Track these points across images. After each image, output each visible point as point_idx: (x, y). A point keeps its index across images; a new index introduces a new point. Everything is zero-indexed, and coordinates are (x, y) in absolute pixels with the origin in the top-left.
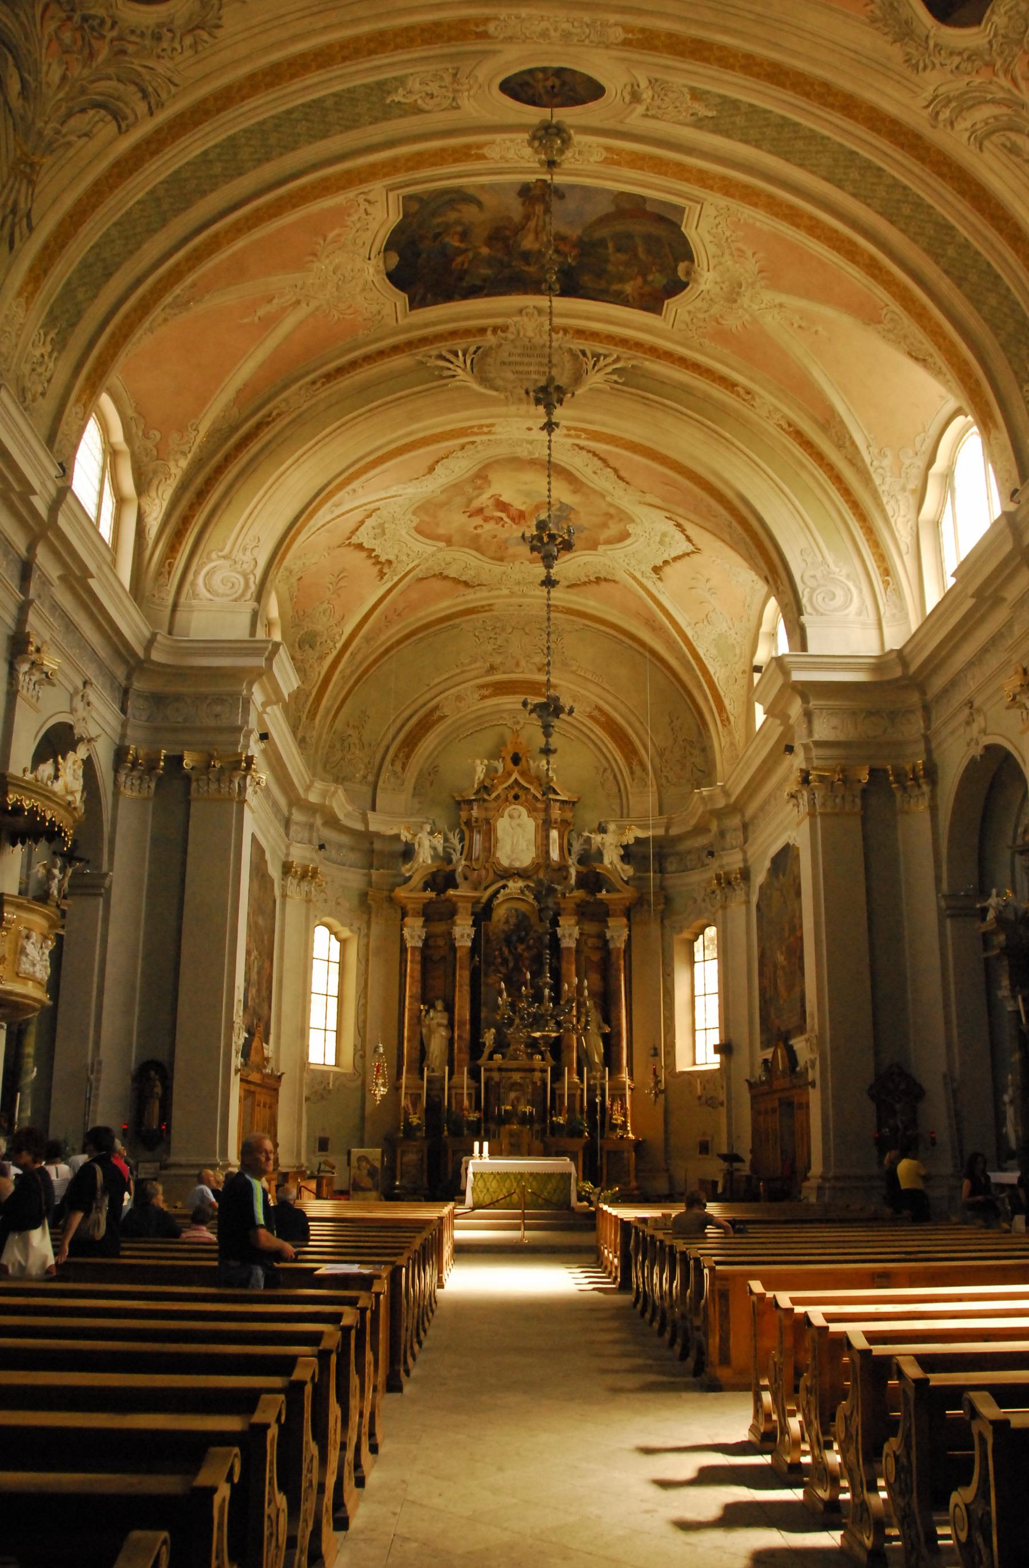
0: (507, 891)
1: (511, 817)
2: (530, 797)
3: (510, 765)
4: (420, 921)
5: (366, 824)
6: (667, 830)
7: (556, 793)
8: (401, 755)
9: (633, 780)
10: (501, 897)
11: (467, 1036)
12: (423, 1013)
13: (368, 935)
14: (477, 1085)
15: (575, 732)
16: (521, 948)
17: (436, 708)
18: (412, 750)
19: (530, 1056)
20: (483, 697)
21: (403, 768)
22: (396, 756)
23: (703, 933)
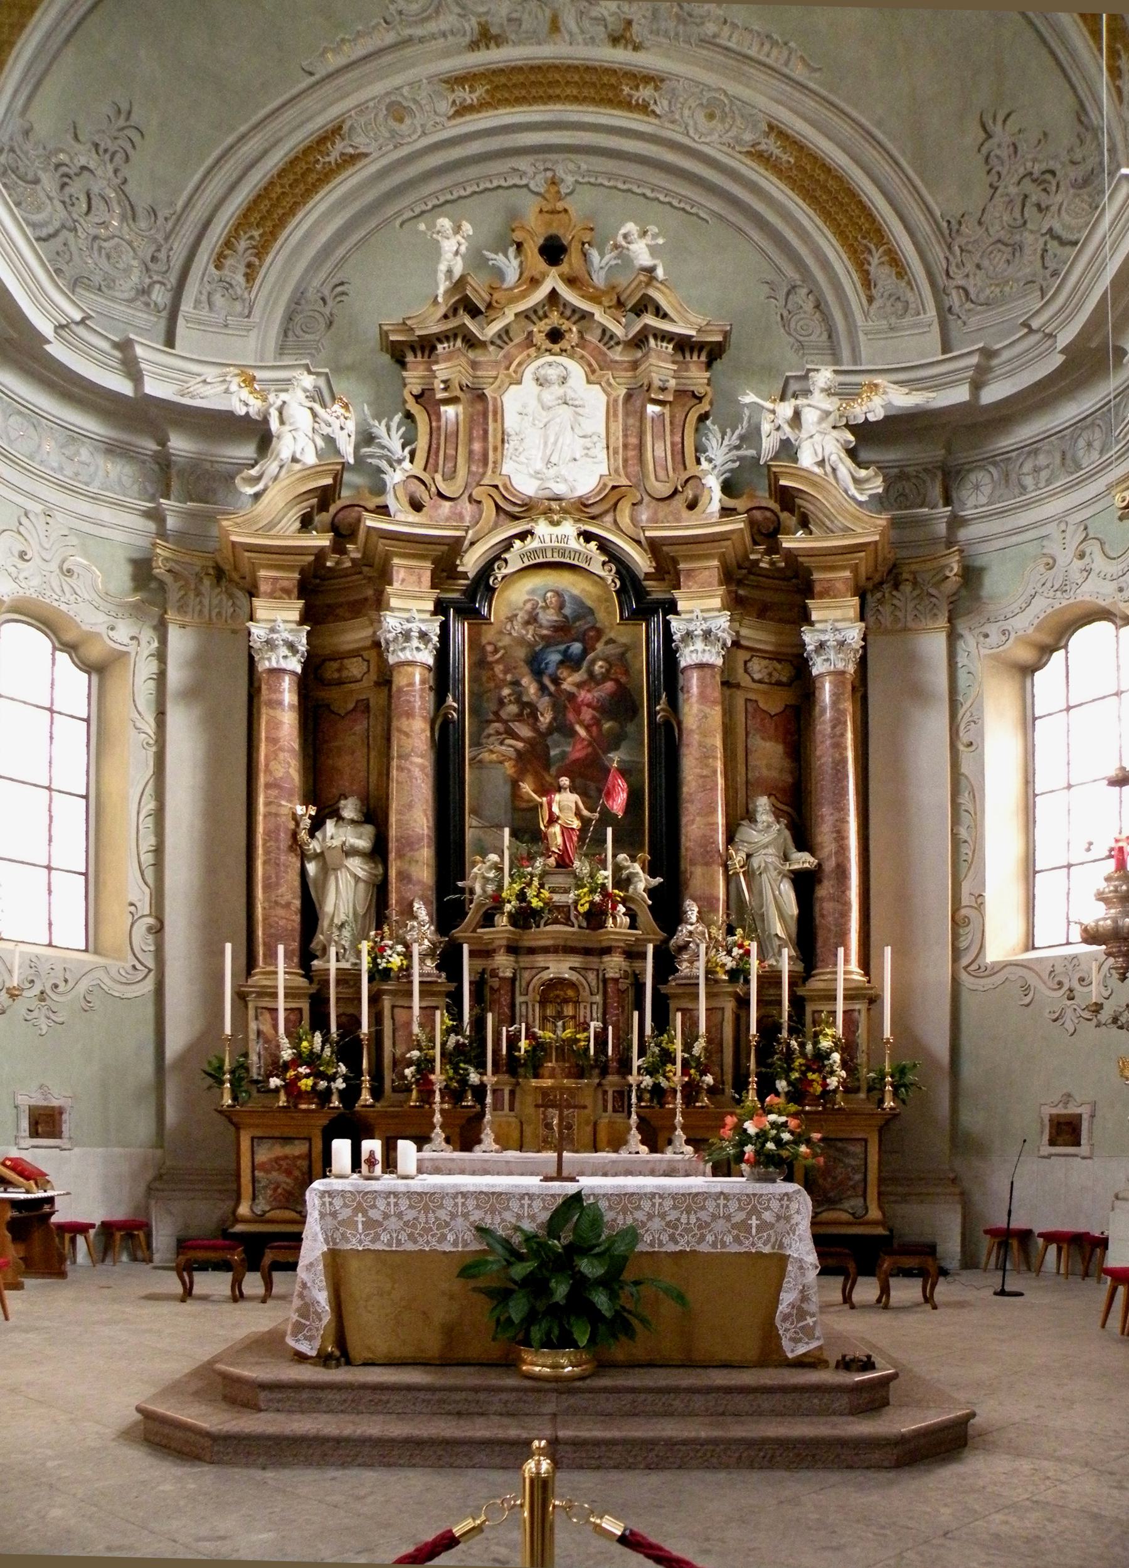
0: (532, 544)
1: (541, 382)
2: (593, 338)
4: (292, 611)
10: (514, 561)
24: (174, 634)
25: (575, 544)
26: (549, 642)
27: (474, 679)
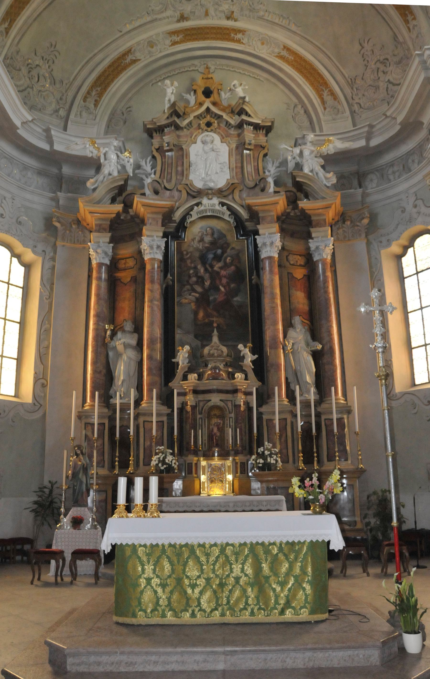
0: (201, 208)
2: (223, 125)
3: (202, 98)
5: (51, 142)
6: (368, 140)
7: (247, 114)
8: (94, 93)
9: (325, 109)
10: (194, 215)
11: (158, 356)
12: (109, 333)
13: (53, 259)
14: (169, 411)
15: (266, 75)
16: (217, 266)
17: (129, 52)
18: (105, 89)
19: (231, 376)
20: (174, 43)
21: (96, 105)
22: (89, 93)
23: (413, 246)
24: (59, 250)
25: (218, 207)
26: (208, 250)
27: (179, 266)
